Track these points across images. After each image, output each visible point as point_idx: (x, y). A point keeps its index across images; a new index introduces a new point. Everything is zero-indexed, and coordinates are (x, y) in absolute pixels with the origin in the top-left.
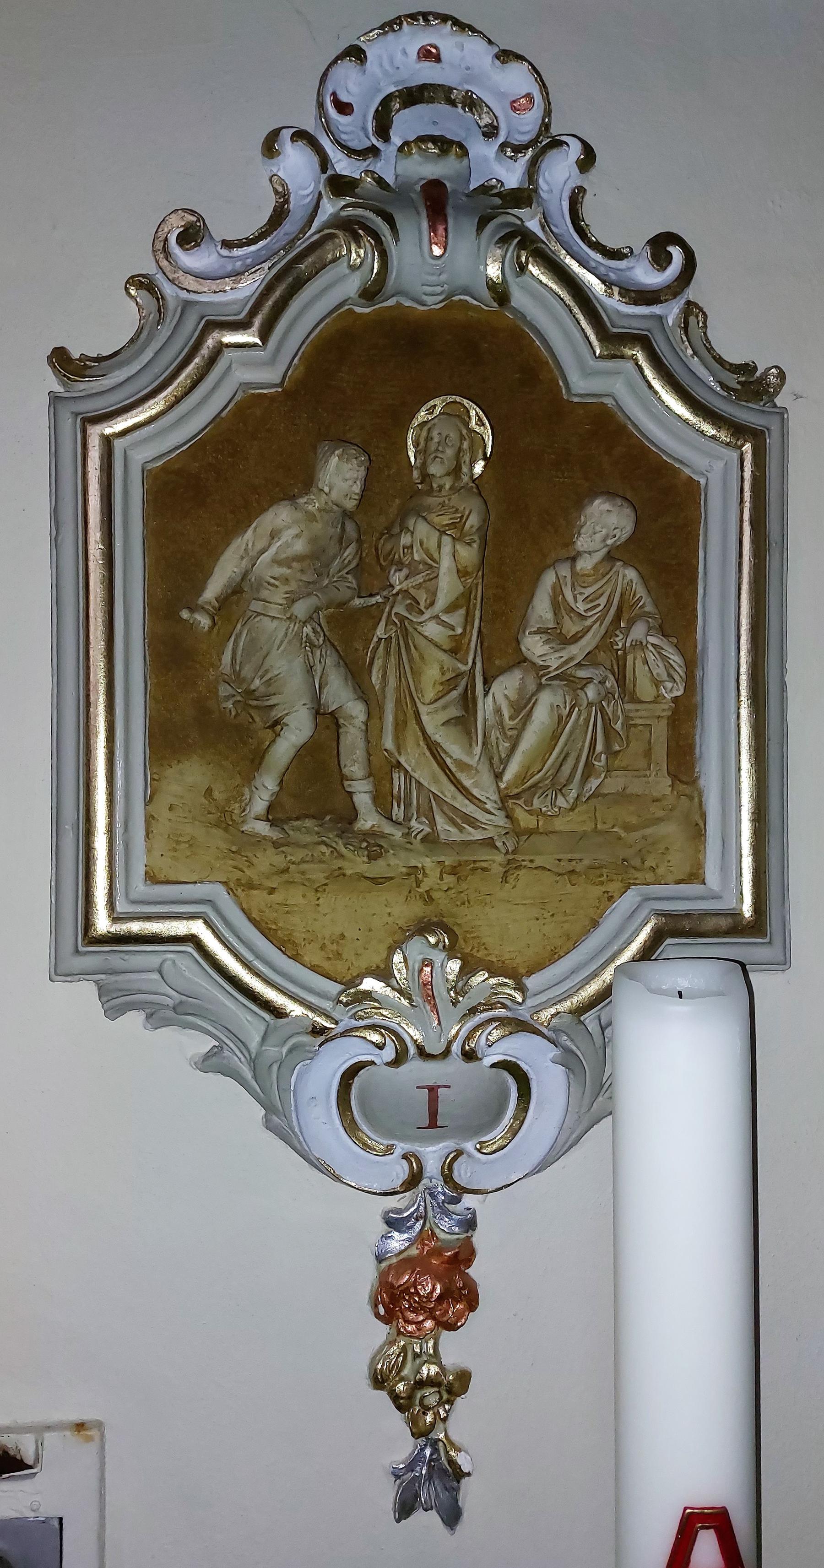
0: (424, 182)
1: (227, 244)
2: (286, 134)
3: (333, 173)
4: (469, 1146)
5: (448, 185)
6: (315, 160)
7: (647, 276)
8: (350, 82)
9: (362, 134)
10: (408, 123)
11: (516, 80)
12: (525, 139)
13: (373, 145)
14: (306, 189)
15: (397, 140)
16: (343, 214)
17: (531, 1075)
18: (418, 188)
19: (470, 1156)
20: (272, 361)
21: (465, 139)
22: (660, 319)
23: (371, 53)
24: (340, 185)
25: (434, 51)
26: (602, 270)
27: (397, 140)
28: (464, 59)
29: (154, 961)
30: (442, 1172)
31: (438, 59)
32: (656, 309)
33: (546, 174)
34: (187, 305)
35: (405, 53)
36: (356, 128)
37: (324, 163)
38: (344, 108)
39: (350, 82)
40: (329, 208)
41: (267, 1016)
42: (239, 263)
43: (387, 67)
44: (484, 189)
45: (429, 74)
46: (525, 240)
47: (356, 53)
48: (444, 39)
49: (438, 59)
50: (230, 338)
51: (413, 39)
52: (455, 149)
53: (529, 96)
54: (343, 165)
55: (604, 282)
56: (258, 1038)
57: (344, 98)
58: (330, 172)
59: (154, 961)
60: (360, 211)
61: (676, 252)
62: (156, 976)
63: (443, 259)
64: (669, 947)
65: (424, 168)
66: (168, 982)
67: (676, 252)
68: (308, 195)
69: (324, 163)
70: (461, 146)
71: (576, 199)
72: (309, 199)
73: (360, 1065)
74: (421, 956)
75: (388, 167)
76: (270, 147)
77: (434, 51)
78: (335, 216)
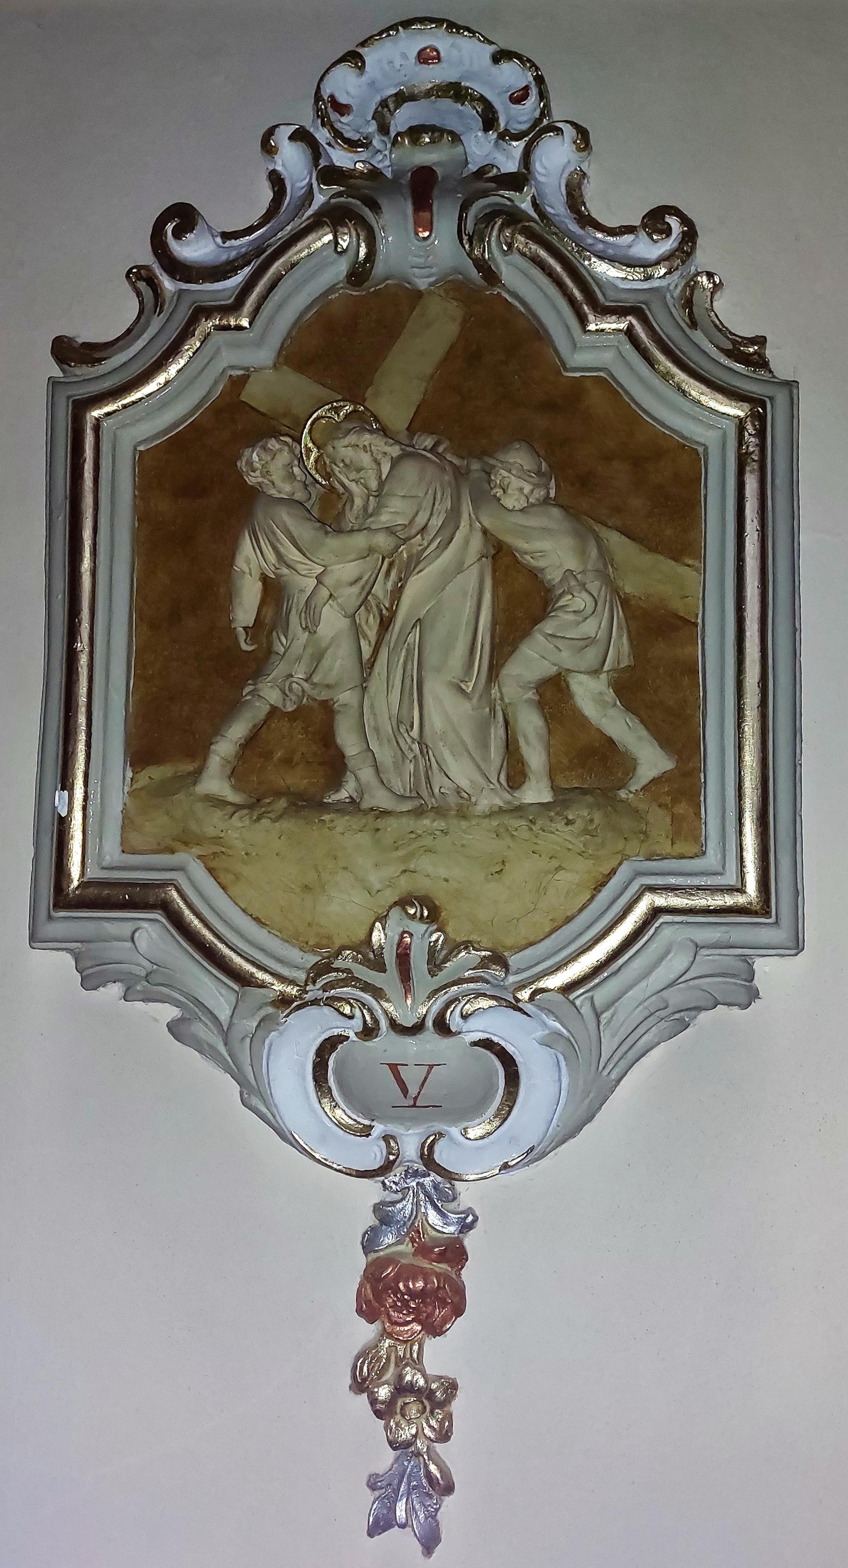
4: (455, 1131)
11: (512, 75)
12: (524, 127)
17: (518, 1059)
19: (452, 1140)
23: (371, 55)
24: (331, 175)
30: (422, 1156)
35: (404, 56)
39: (344, 84)
44: (480, 173)
47: (354, 58)
48: (442, 41)
51: (410, 43)
52: (447, 138)
53: (526, 89)
56: (228, 1012)
57: (342, 99)
58: (323, 163)
59: (126, 929)
74: (402, 929)
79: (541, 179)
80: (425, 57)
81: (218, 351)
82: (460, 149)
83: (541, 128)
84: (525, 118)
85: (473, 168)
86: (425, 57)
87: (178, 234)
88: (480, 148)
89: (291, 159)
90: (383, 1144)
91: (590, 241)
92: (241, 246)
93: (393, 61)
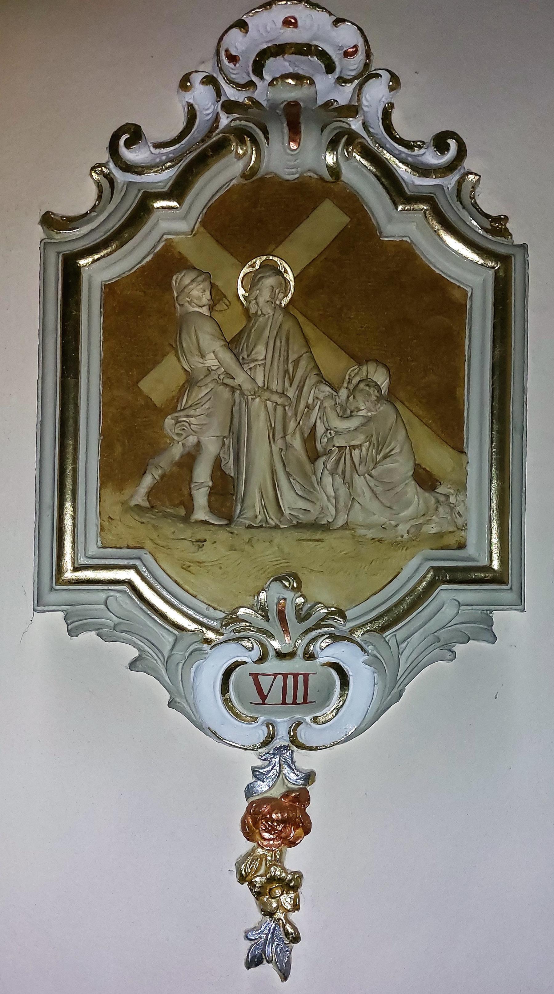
0: (285, 103)
1: (158, 146)
3: (226, 99)
5: (302, 104)
7: (432, 158)
8: (236, 41)
9: (245, 75)
10: (276, 66)
11: (347, 36)
15: (268, 78)
16: (233, 124)
18: (282, 106)
20: (185, 218)
21: (313, 75)
22: (441, 187)
23: (251, 22)
24: (230, 107)
25: (293, 21)
27: (268, 78)
28: (313, 25)
29: (103, 596)
31: (295, 25)
33: (367, 96)
34: (130, 184)
38: (233, 59)
39: (236, 41)
40: (224, 120)
41: (176, 632)
42: (164, 158)
43: (262, 31)
45: (290, 36)
46: (352, 138)
49: (295, 25)
51: (279, 13)
53: (355, 46)
54: (231, 93)
56: (169, 647)
58: (223, 99)
59: (103, 596)
60: (243, 122)
61: (452, 143)
63: (297, 151)
64: (443, 592)
66: (111, 609)
67: (452, 143)
70: (310, 78)
71: (387, 115)
73: (238, 663)
75: (262, 93)
76: (185, 84)
77: (293, 21)
78: (228, 126)
79: (365, 109)
80: (289, 22)
81: (157, 224)
82: (312, 88)
83: (367, 75)
84: (355, 67)
85: (320, 102)
86: (289, 22)
87: (128, 144)
88: (325, 88)
89: (201, 96)
90: (265, 728)
91: (397, 152)
92: (170, 152)
93: (267, 26)
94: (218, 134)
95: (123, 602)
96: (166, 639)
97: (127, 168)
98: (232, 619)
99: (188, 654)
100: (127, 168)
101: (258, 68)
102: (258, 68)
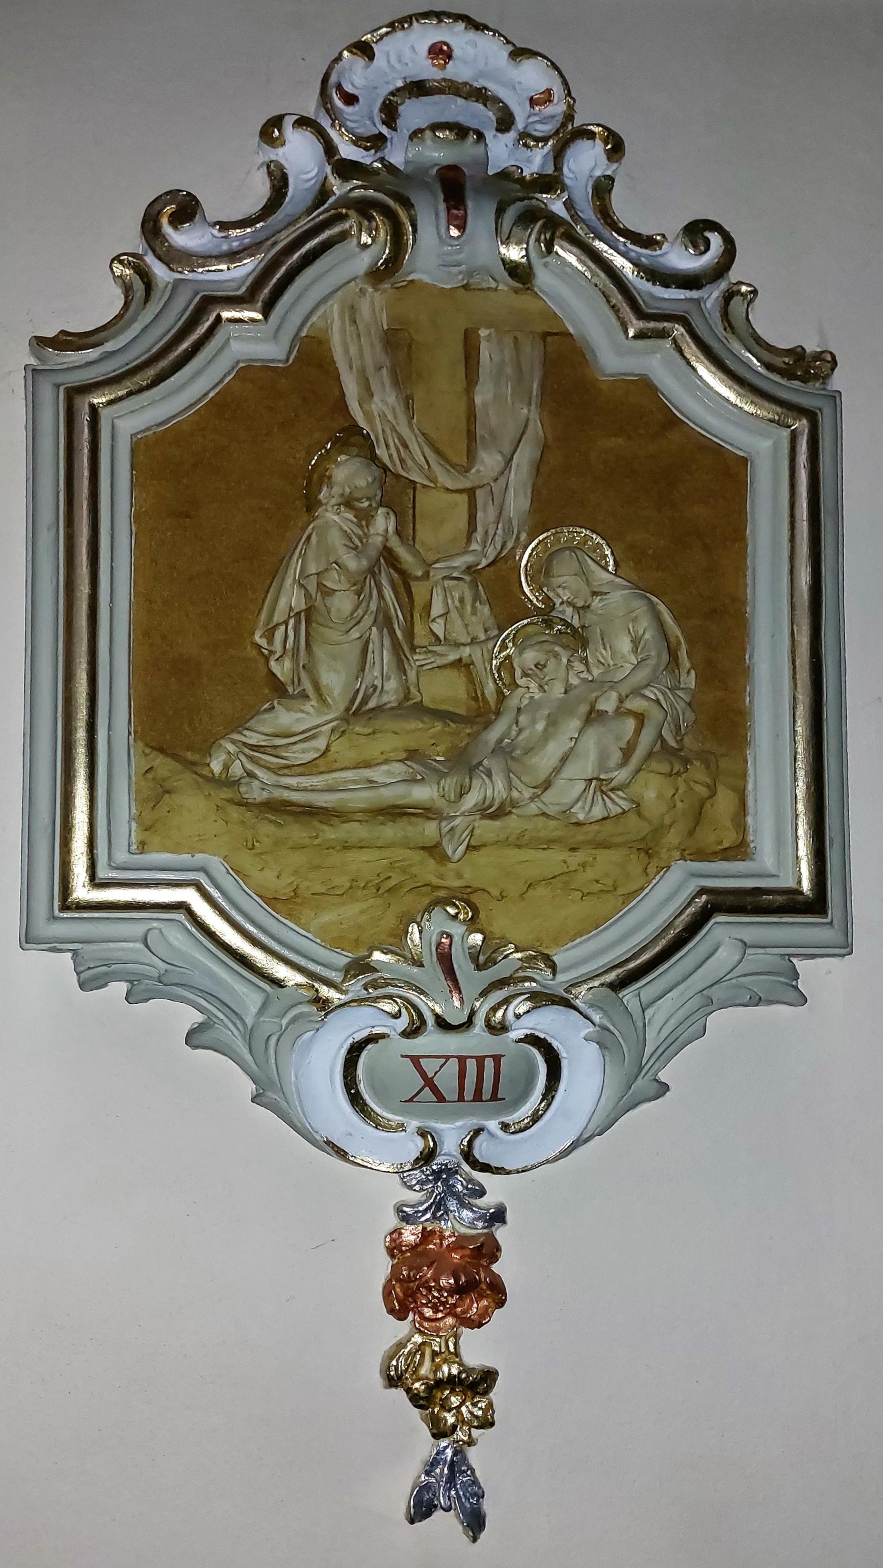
1: (224, 226)
2: (289, 121)
6: (320, 149)
7: (682, 259)
13: (380, 133)
14: (308, 172)
26: (633, 254)
32: (694, 294)
33: (572, 160)
36: (364, 117)
37: (330, 149)
39: (356, 75)
50: (226, 315)
54: (348, 151)
55: (635, 264)
62: (140, 946)
65: (437, 153)
66: (153, 950)
68: (311, 180)
69: (330, 149)
72: (313, 182)
79: (567, 182)
82: (481, 148)
93: (406, 54)
94: (327, 210)
95: (176, 937)
96: (248, 997)
97: (173, 257)
98: (360, 967)
99: (284, 1022)
100: (173, 257)
101: (390, 112)
102: (390, 112)
